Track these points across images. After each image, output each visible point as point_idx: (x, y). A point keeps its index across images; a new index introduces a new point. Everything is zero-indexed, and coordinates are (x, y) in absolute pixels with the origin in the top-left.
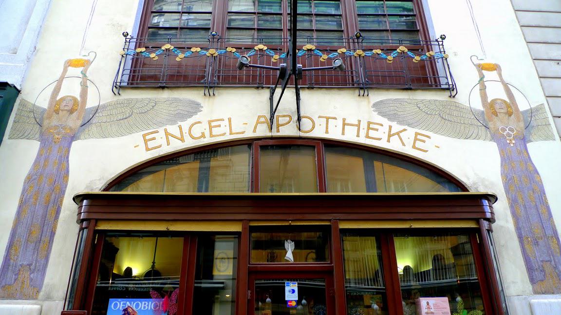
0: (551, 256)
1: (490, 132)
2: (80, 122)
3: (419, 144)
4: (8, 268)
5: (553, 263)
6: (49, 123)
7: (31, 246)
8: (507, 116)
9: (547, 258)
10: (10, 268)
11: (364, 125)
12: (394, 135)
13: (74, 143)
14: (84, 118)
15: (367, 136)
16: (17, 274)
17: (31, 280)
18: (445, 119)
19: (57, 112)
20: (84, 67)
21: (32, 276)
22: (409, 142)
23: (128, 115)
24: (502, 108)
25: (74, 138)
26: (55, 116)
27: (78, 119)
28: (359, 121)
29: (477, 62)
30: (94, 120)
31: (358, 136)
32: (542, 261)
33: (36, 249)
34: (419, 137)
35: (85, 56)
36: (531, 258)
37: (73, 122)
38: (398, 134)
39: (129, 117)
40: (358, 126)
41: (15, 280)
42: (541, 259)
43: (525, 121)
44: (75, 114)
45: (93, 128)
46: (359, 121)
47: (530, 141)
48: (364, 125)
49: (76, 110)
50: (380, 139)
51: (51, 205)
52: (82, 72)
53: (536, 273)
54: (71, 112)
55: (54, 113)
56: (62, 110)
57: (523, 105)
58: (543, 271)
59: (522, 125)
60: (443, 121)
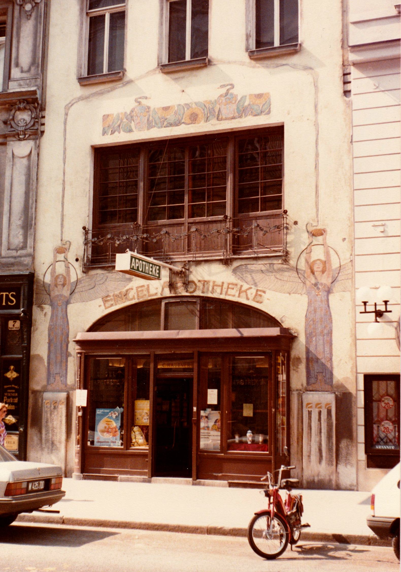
0: (324, 370)
1: (306, 288)
2: (69, 292)
3: (258, 299)
4: (50, 376)
5: (324, 374)
6: (54, 294)
7: (58, 365)
8: (321, 273)
9: (321, 371)
10: (51, 375)
11: (225, 286)
12: (243, 292)
13: (68, 306)
14: (71, 290)
15: (226, 294)
16: (55, 378)
17: (61, 381)
18: (277, 279)
19: (56, 286)
20: (65, 252)
21: (61, 379)
22: (251, 297)
23: (93, 286)
24: (319, 268)
25: (68, 302)
26: (56, 289)
27: (68, 290)
28: (223, 283)
29: (310, 229)
30: (76, 291)
31: (221, 294)
32: (318, 373)
33: (61, 366)
34: (259, 293)
35: (64, 244)
36: (311, 371)
37: (66, 292)
38: (246, 291)
39: (94, 287)
40: (222, 286)
41: (54, 381)
42: (317, 371)
43: (333, 277)
44: (66, 287)
45: (76, 296)
46: (223, 283)
47: (333, 293)
48: (225, 286)
49: (66, 284)
50: (234, 296)
51: (63, 342)
52: (64, 257)
53: (312, 379)
54: (64, 285)
55: (55, 287)
56: (59, 285)
57: (335, 264)
58: (317, 378)
59: (330, 280)
60: (276, 280)
